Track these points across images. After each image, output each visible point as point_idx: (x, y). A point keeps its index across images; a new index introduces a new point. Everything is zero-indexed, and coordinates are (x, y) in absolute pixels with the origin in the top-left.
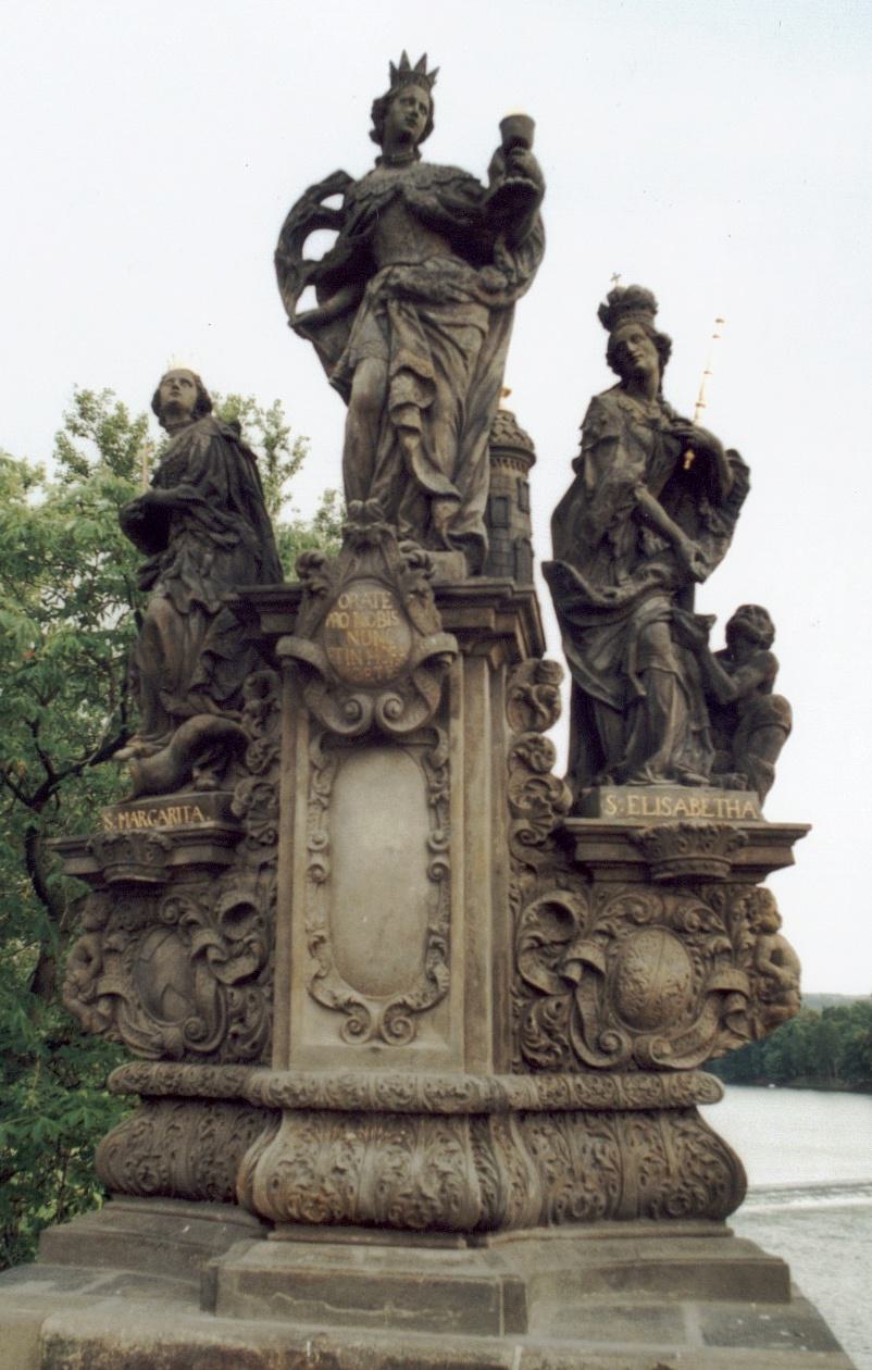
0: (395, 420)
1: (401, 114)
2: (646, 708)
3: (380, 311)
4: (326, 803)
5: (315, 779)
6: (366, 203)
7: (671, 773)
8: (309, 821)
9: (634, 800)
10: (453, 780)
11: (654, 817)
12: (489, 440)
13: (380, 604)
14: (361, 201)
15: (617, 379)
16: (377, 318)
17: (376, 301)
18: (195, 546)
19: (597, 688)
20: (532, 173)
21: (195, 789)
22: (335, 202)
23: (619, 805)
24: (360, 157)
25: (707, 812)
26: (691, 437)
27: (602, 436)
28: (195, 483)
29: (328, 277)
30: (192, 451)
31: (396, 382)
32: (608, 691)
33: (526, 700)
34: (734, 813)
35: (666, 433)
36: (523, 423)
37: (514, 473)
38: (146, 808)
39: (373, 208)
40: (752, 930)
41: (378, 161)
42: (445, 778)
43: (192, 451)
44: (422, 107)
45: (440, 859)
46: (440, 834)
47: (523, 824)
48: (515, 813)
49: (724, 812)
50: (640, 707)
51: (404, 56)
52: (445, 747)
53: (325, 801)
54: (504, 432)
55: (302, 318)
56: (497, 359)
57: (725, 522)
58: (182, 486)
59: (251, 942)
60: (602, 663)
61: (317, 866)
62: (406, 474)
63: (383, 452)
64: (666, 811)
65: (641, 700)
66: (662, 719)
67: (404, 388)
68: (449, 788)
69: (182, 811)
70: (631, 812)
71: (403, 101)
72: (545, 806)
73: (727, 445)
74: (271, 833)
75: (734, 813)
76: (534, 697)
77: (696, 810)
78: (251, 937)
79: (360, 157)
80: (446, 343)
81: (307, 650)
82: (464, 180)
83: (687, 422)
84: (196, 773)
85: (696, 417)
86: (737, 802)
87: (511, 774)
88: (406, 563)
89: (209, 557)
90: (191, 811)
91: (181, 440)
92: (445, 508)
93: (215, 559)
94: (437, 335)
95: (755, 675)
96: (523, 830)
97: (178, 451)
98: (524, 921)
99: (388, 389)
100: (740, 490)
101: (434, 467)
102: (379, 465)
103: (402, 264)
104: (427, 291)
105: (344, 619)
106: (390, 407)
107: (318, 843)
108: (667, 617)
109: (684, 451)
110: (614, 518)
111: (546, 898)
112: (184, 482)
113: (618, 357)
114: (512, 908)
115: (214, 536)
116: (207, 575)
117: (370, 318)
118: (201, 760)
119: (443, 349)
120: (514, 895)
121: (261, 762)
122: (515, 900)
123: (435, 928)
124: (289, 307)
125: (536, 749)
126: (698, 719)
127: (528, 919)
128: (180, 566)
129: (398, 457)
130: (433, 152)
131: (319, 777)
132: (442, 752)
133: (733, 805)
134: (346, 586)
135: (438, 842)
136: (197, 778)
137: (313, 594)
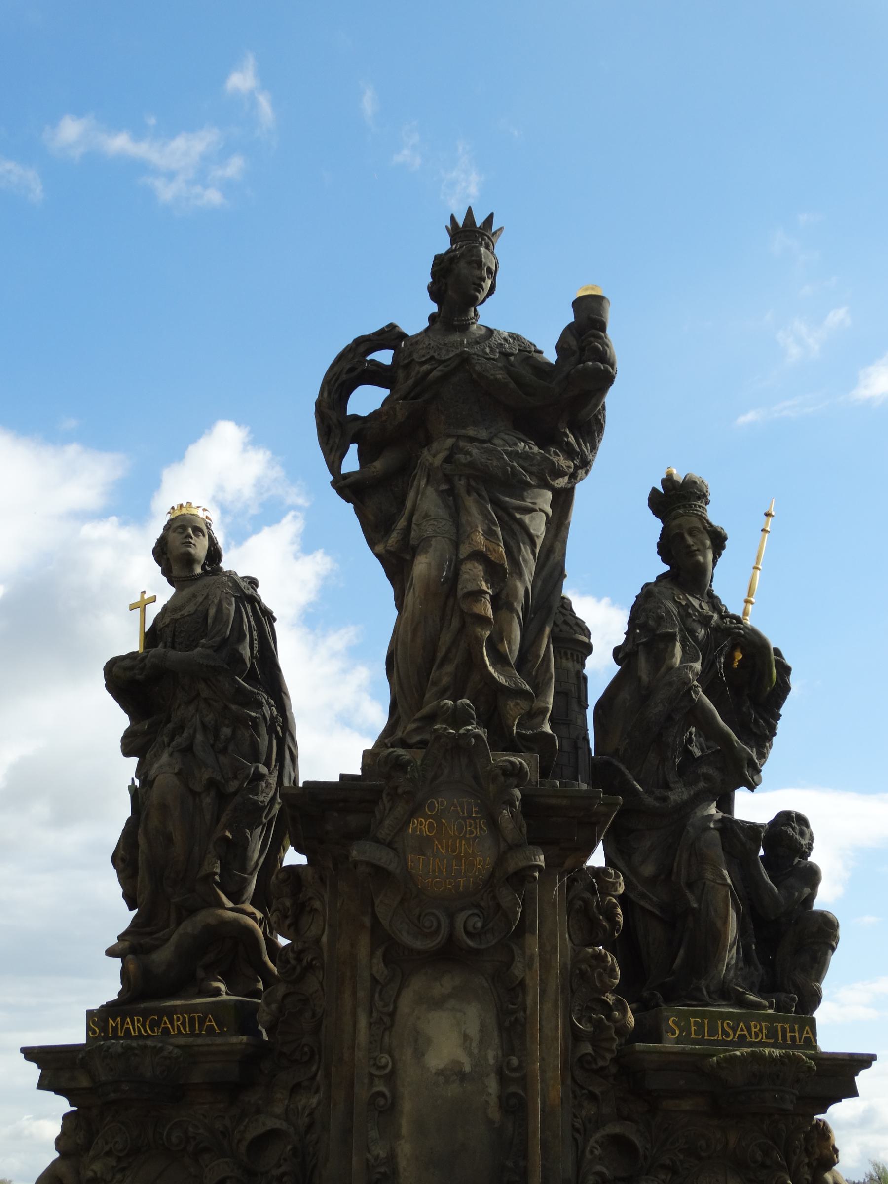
0: (464, 607)
1: (461, 272)
3: (444, 487)
4: (385, 1022)
5: (377, 996)
6: (426, 367)
7: (726, 994)
8: (371, 1043)
9: (696, 1023)
10: (529, 1002)
12: (552, 631)
13: (470, 812)
14: (423, 363)
15: (667, 568)
16: (441, 493)
19: (643, 896)
20: (604, 357)
22: (385, 357)
23: (679, 1032)
24: (415, 314)
27: (658, 632)
28: (218, 649)
29: (369, 434)
30: (212, 612)
31: (467, 567)
32: (655, 899)
34: (793, 1038)
35: (717, 629)
37: (569, 664)
38: (145, 1014)
39: (436, 374)
40: (809, 1165)
41: (432, 318)
42: (520, 999)
43: (212, 612)
44: (489, 270)
45: (512, 1089)
46: (515, 1061)
47: (587, 1048)
48: (576, 1036)
53: (386, 1019)
54: (566, 622)
55: (349, 480)
56: (558, 545)
57: (767, 722)
58: (199, 649)
59: (284, 1174)
60: (648, 870)
61: (381, 1094)
62: (472, 662)
63: (446, 638)
64: (728, 1035)
66: (717, 937)
67: (475, 576)
68: (525, 1011)
69: (192, 1020)
70: (693, 1036)
71: (469, 263)
73: (773, 644)
74: (306, 1049)
75: (793, 1038)
77: (757, 1036)
78: (281, 1170)
79: (415, 314)
80: (516, 528)
82: (528, 354)
83: (739, 620)
84: (200, 974)
85: (745, 613)
86: (796, 1027)
88: (500, 772)
89: (226, 731)
90: (202, 1021)
91: (194, 596)
92: (517, 704)
93: (234, 732)
94: (506, 518)
95: (807, 891)
96: (586, 1054)
97: (190, 608)
98: (588, 1155)
99: (456, 575)
100: (783, 689)
101: (500, 659)
102: (440, 654)
103: (471, 439)
105: (430, 824)
106: (460, 593)
107: (384, 1067)
108: (719, 825)
109: (733, 648)
111: (615, 1129)
113: (666, 549)
114: (575, 1139)
115: (234, 707)
116: (224, 751)
117: (430, 492)
119: (513, 534)
120: (577, 1125)
121: (294, 968)
122: (578, 1130)
123: (510, 1164)
124: (334, 465)
127: (592, 1152)
128: (192, 737)
130: (494, 315)
131: (380, 993)
132: (518, 970)
133: (792, 1030)
135: (514, 1070)
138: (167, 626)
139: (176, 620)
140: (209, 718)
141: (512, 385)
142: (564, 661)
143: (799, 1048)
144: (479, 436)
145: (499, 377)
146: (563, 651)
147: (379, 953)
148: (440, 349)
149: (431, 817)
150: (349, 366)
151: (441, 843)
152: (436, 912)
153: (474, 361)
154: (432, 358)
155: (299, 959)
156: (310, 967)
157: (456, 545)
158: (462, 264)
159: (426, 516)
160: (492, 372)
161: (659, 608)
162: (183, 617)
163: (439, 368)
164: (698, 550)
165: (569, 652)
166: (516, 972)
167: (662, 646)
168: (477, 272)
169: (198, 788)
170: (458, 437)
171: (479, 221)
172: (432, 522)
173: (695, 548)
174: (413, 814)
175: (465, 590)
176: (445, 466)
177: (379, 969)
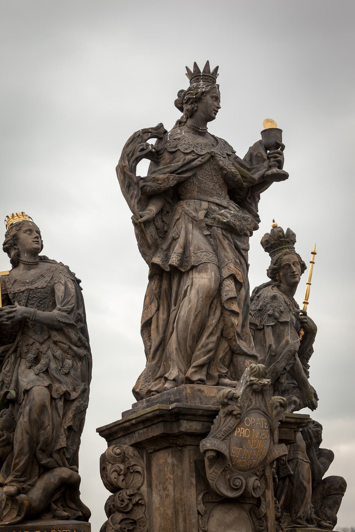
0: (226, 306)
1: (200, 99)
2: (291, 482)
7: (309, 521)
17: (204, 225)
18: (58, 353)
21: (55, 517)
26: (306, 323)
27: (281, 320)
42: (265, 524)
51: (208, 64)
52: (264, 506)
63: (213, 321)
65: (290, 476)
67: (229, 287)
71: (212, 97)
81: (223, 448)
84: (54, 507)
88: (278, 404)
97: (40, 284)
104: (238, 228)
106: (225, 298)
110: (285, 369)
112: (59, 310)
115: (75, 348)
116: (67, 374)
118: (57, 496)
121: (128, 504)
129: (220, 326)
132: (263, 509)
134: (248, 413)
136: (56, 510)
137: (230, 414)
138: (23, 292)
139: (31, 290)
140: (58, 353)
141: (239, 176)
144: (222, 204)
145: (233, 170)
147: (200, 497)
148: (197, 147)
149: (248, 427)
150: (141, 147)
151: (251, 442)
152: (240, 477)
153: (218, 159)
154: (193, 151)
155: (130, 500)
156: (137, 504)
157: (219, 268)
158: (208, 97)
159: (199, 249)
160: (229, 167)
161: (281, 306)
162: (37, 288)
163: (200, 159)
166: (263, 510)
167: (282, 328)
168: (216, 103)
169: (55, 396)
170: (209, 202)
171: (212, 69)
172: (204, 253)
173: (296, 273)
174: (238, 426)
175: (228, 297)
176: (206, 220)
177: (201, 508)
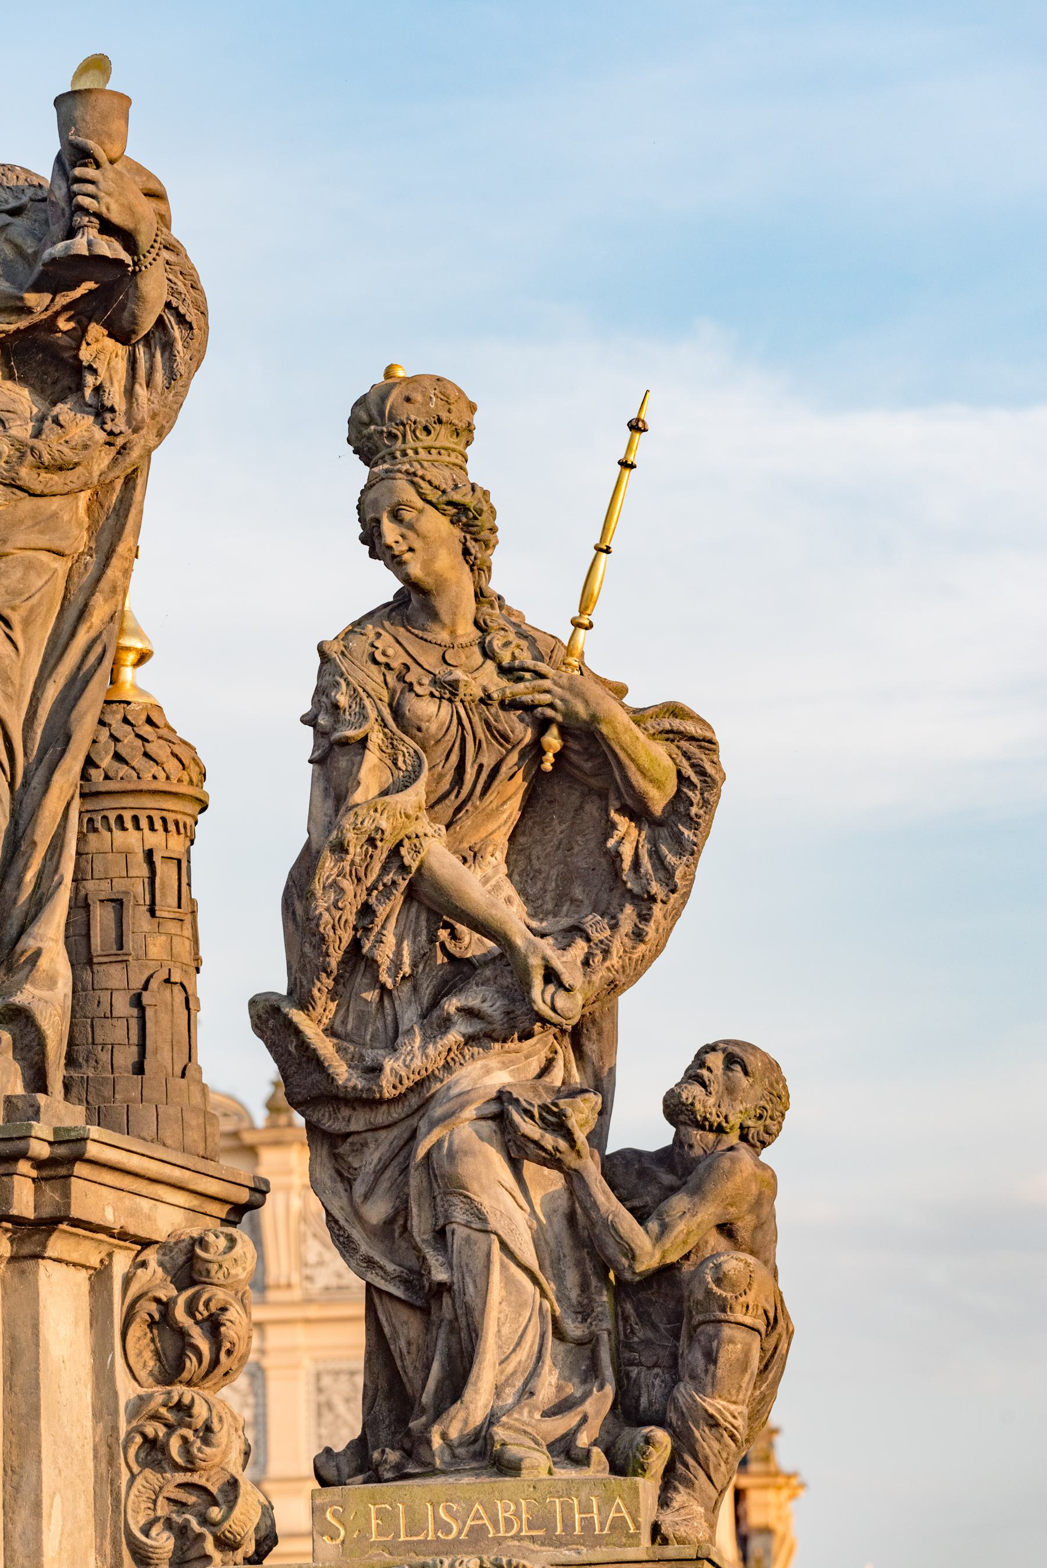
11: (425, 1542)
25: (531, 1527)
32: (390, 1267)
33: (163, 1320)
36: (181, 720)
49: (568, 1525)
50: (446, 1300)
65: (443, 1288)
72: (200, 1537)
76: (180, 1314)
87: (133, 1477)
125: (181, 1424)
126: (584, 1312)
133: (586, 1508)
142: (118, 833)
143: (598, 1541)
146: (112, 816)
164: (411, 550)
165: (127, 816)
